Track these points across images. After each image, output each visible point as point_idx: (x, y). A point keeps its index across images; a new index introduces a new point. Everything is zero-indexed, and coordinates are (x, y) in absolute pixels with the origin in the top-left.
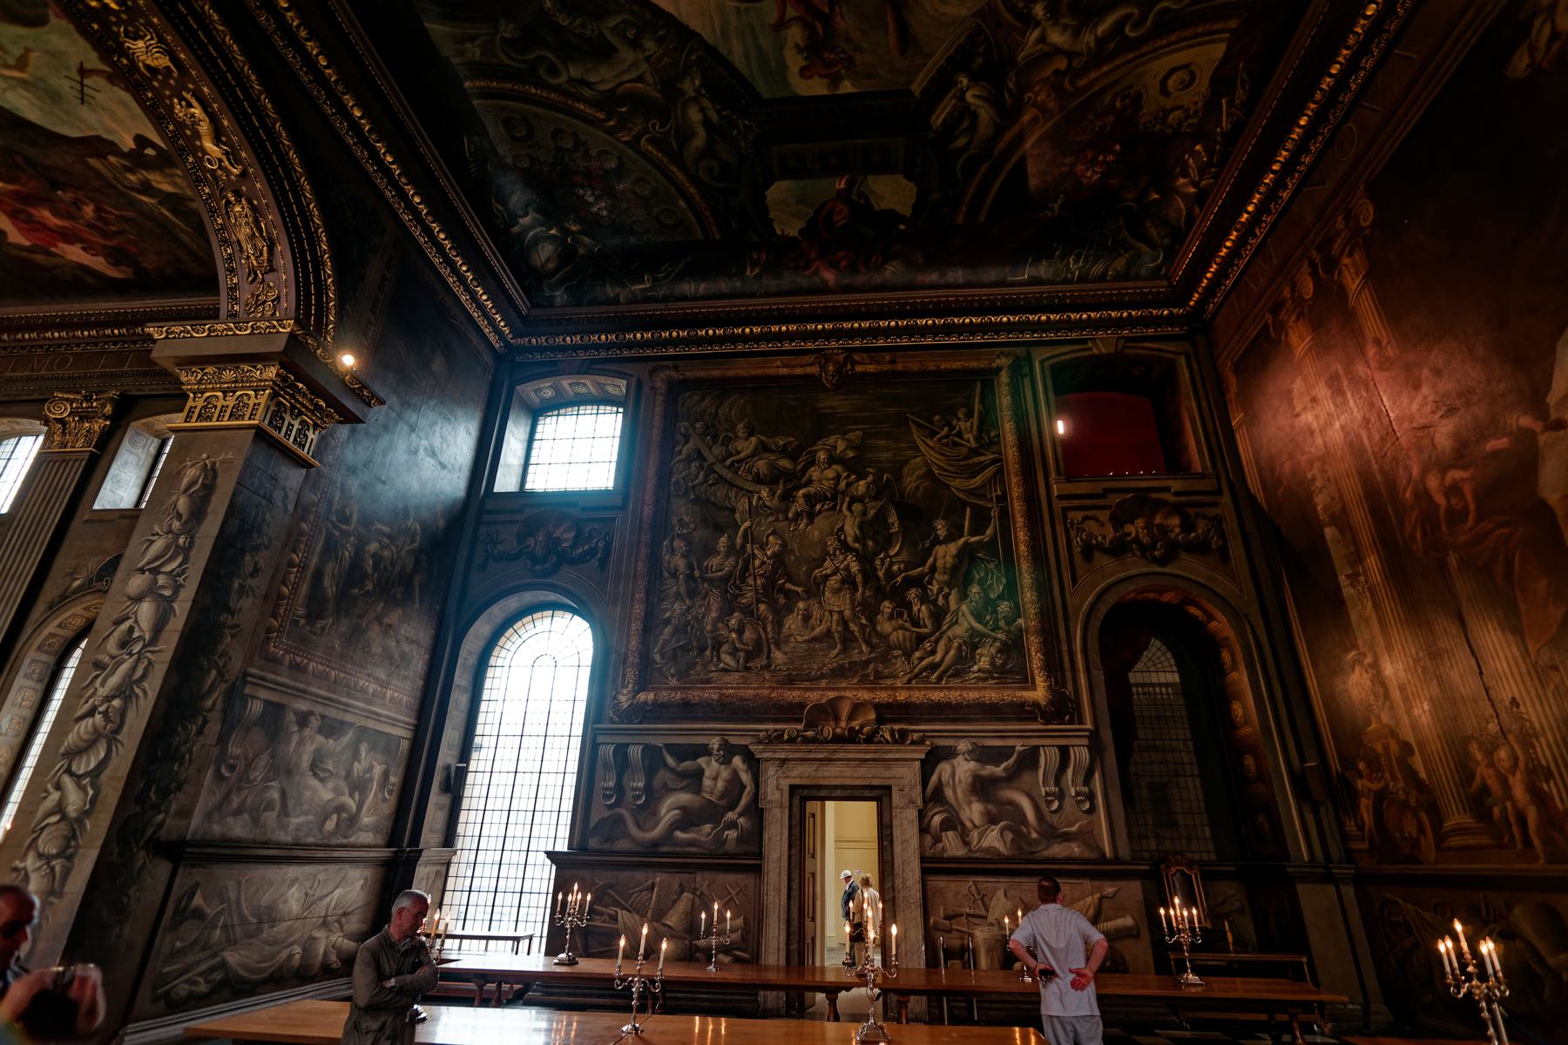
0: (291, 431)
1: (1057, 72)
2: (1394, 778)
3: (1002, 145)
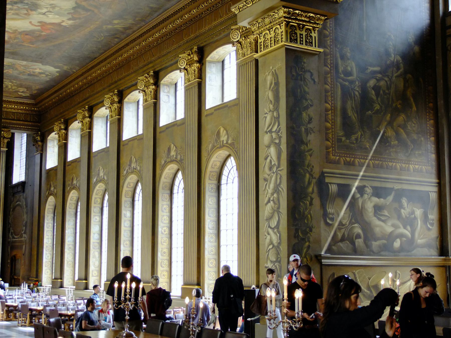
0: (302, 38)
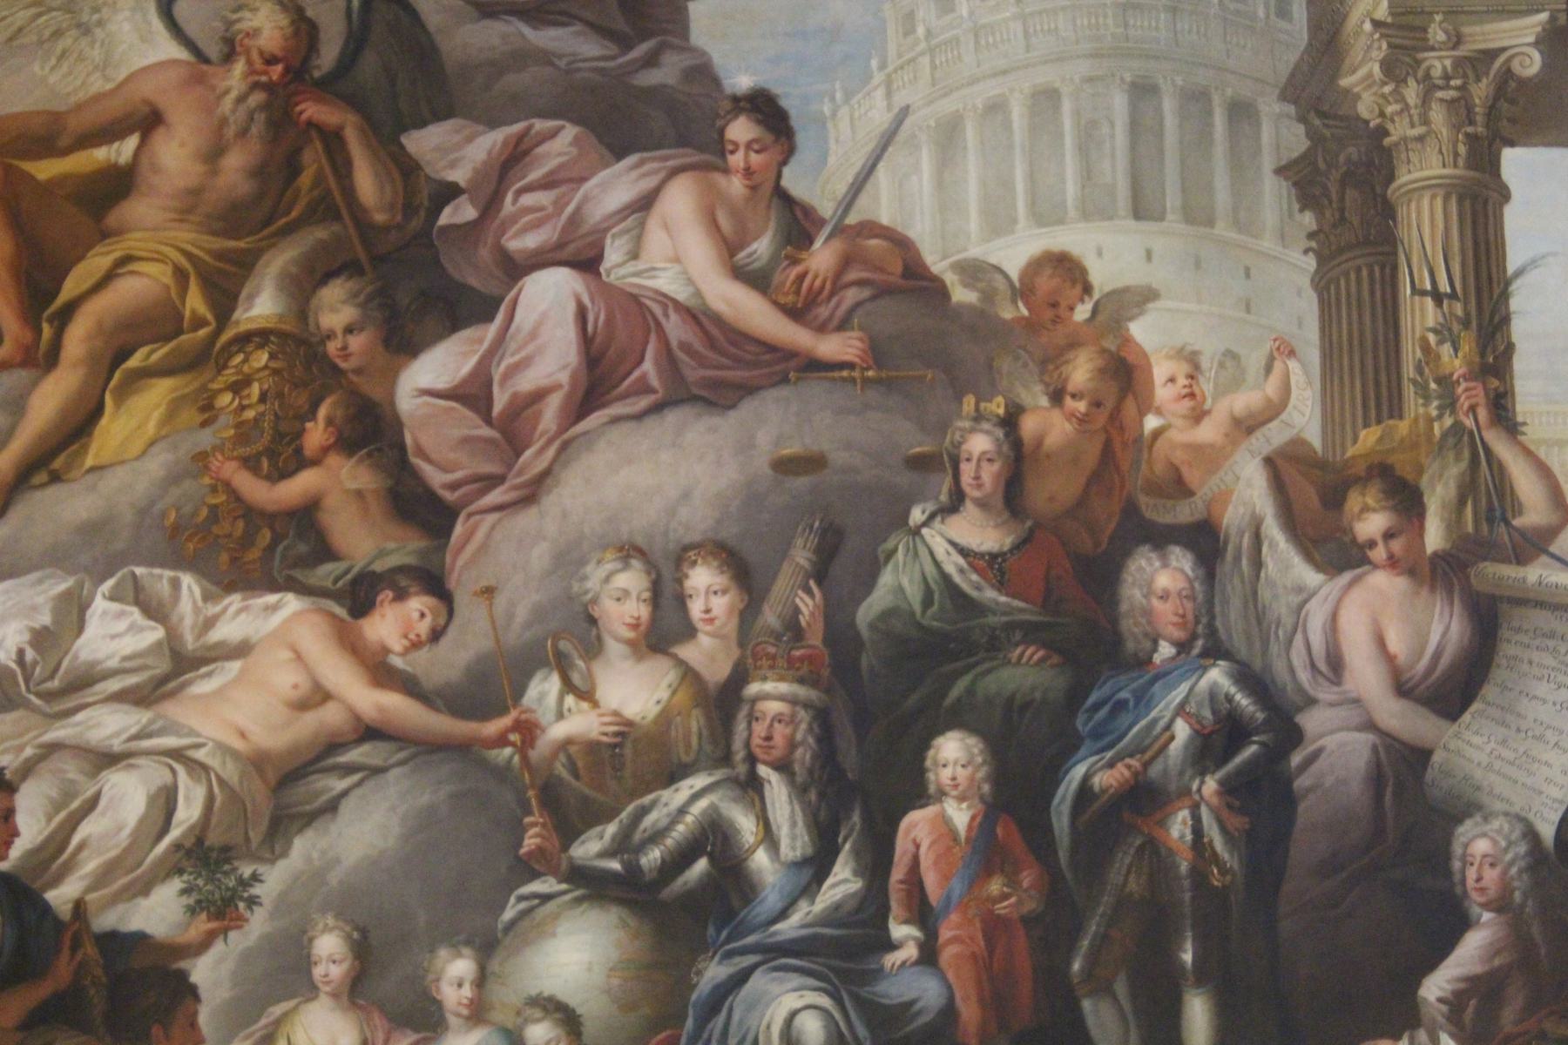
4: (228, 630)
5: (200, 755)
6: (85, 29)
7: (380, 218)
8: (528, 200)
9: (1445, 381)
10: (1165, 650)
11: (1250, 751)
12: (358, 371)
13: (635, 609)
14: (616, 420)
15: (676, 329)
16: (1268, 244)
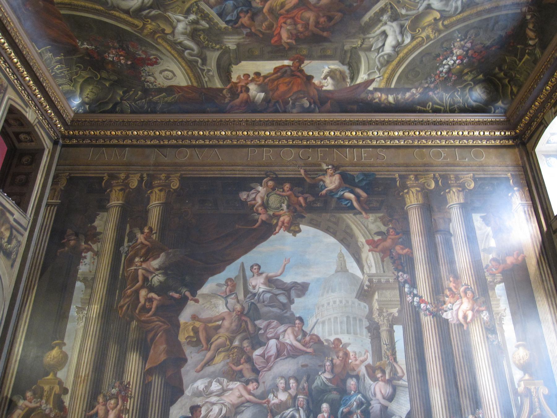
1: (163, 30)
2: (47, 402)
3: (117, 14)
4: (230, 386)
5: (226, 404)
6: (216, 307)
7: (252, 332)
8: (270, 330)
9: (388, 356)
10: (353, 392)
11: (364, 406)
12: (248, 352)
13: (283, 385)
14: (281, 359)
15: (289, 347)
16: (364, 337)
